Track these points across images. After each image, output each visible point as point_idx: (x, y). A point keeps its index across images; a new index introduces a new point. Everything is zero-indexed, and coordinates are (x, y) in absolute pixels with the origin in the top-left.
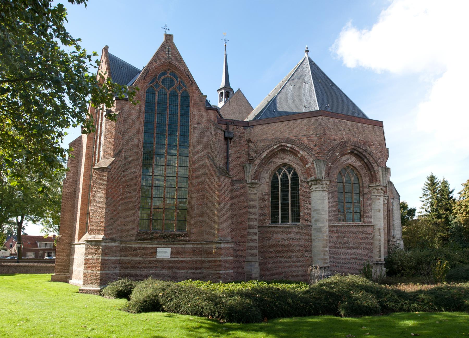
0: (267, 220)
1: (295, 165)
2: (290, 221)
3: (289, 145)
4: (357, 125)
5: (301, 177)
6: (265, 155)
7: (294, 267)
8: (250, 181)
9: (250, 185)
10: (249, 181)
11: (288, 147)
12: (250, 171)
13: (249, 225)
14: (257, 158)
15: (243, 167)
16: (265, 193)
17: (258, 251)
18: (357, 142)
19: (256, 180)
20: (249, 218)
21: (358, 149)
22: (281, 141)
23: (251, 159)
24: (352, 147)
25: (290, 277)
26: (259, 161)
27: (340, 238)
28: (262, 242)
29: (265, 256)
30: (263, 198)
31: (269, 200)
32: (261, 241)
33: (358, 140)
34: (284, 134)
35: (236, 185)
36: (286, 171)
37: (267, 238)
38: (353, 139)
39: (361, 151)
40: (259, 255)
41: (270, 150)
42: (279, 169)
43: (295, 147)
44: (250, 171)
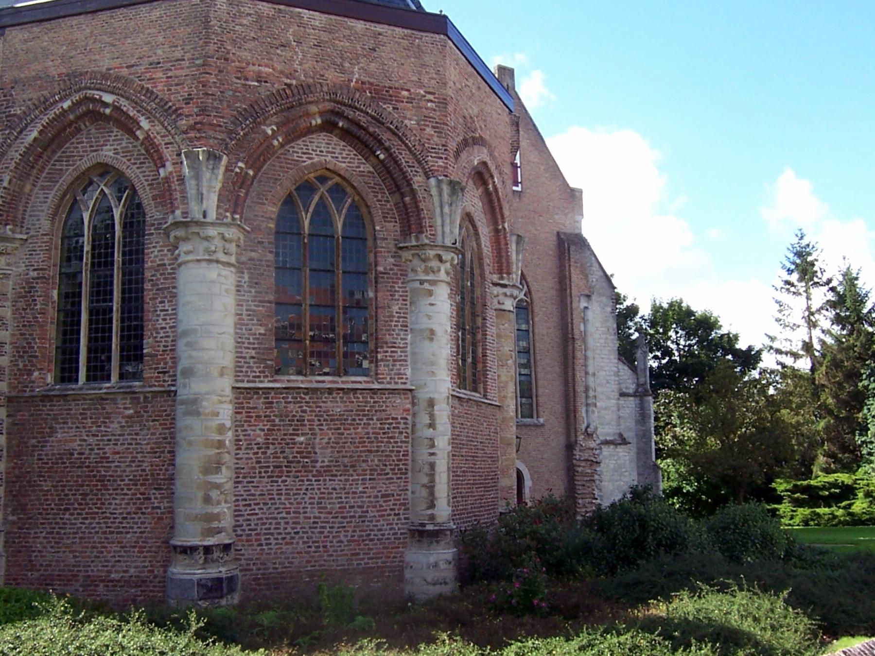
0: (36, 374)
1: (133, 173)
2: (115, 377)
3: (108, 98)
4: (350, 28)
5: (153, 213)
6: (35, 134)
7: (115, 547)
11: (106, 105)
16: (34, 274)
18: (348, 87)
21: (350, 113)
24: (329, 106)
25: (101, 588)
31: (47, 296)
33: (350, 81)
34: (97, 57)
36: (106, 191)
37: (34, 441)
38: (332, 76)
39: (363, 120)
41: (51, 115)
42: (84, 182)
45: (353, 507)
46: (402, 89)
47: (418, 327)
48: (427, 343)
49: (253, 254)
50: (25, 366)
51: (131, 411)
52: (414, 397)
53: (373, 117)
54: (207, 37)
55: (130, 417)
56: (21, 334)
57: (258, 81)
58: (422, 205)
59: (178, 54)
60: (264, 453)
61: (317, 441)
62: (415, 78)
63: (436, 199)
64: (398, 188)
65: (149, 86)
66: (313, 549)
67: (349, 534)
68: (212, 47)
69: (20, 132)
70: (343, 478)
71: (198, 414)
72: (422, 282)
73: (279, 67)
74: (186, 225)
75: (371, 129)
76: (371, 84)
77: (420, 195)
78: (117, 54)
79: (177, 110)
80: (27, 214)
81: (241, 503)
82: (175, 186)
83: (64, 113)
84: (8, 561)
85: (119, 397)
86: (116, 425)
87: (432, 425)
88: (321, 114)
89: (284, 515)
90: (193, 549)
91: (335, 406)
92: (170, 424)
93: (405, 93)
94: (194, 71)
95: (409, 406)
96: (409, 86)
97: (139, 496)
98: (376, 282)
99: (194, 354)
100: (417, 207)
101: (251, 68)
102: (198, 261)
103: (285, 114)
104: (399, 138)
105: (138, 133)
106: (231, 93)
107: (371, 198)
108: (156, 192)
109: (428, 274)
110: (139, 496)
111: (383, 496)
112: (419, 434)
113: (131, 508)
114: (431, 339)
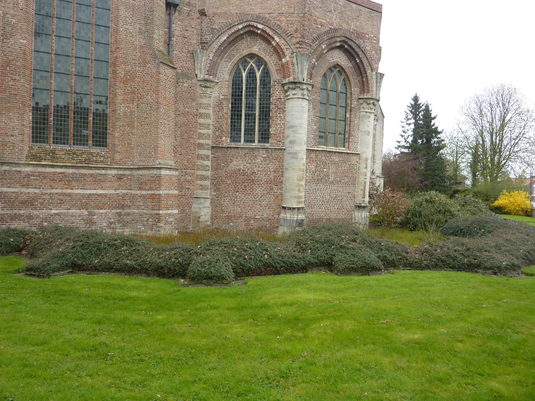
0: (224, 138)
1: (267, 58)
2: (256, 141)
3: (260, 26)
4: (351, 7)
5: (275, 76)
6: (225, 38)
7: (258, 206)
8: (202, 77)
9: (202, 83)
10: (201, 76)
11: (259, 29)
12: (203, 60)
13: (199, 143)
14: (213, 42)
15: (193, 55)
17: (210, 182)
18: (350, 31)
19: (210, 75)
20: (200, 133)
21: (350, 42)
22: (249, 18)
23: (204, 43)
24: (343, 39)
25: (252, 221)
26: (216, 47)
27: (319, 168)
28: (216, 169)
29: (219, 190)
30: (219, 104)
31: (228, 107)
32: (216, 168)
33: (350, 29)
34: (254, 8)
35: (181, 80)
36: (254, 65)
37: (223, 164)
38: (345, 26)
39: (354, 46)
40: (211, 189)
41: (233, 30)
42: (244, 61)
43: (268, 30)
44: (203, 60)
45: (339, 196)
46: (367, 34)
47: (364, 130)
48: (367, 136)
49: (314, 97)
50: (219, 134)
51: (266, 155)
52: (360, 157)
53: (357, 45)
54: (305, 5)
55: (265, 157)
56: (217, 122)
57: (321, 26)
58: (370, 82)
59: (292, 11)
60: (314, 174)
61: (330, 171)
62: (370, 30)
63: (375, 80)
64: (361, 74)
65: (279, 23)
66: (327, 211)
67: (338, 206)
68: (307, 9)
69: (219, 36)
70: (337, 185)
71: (297, 158)
72: (366, 112)
73: (328, 20)
74: (296, 83)
75: (356, 50)
76: (357, 31)
77: (369, 78)
78: (263, 8)
79: (291, 35)
80: (218, 72)
81: (307, 192)
82: (290, 66)
83: (239, 30)
84: (212, 210)
85: (260, 150)
86: (259, 160)
87: (366, 168)
88: (340, 41)
89: (319, 198)
90: (294, 208)
91: (336, 158)
92: (281, 161)
93: (367, 36)
94: (299, 19)
95: (358, 160)
96: (369, 33)
97: (268, 188)
98: (351, 111)
99: (296, 135)
100: (368, 83)
101: (319, 20)
102: (299, 98)
103: (329, 40)
104: (365, 54)
105: (273, 42)
106: (312, 30)
107: (351, 77)
108: (277, 68)
109: (369, 110)
110: (268, 188)
111: (349, 193)
112: (361, 171)
113: (265, 192)
114: (368, 135)
